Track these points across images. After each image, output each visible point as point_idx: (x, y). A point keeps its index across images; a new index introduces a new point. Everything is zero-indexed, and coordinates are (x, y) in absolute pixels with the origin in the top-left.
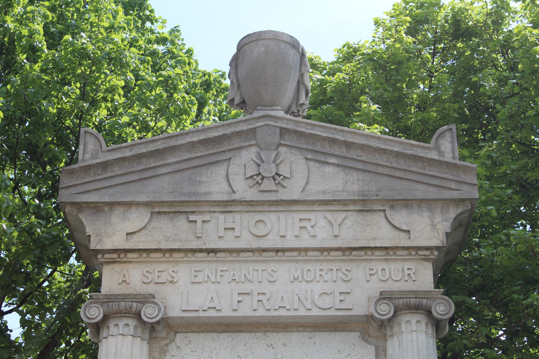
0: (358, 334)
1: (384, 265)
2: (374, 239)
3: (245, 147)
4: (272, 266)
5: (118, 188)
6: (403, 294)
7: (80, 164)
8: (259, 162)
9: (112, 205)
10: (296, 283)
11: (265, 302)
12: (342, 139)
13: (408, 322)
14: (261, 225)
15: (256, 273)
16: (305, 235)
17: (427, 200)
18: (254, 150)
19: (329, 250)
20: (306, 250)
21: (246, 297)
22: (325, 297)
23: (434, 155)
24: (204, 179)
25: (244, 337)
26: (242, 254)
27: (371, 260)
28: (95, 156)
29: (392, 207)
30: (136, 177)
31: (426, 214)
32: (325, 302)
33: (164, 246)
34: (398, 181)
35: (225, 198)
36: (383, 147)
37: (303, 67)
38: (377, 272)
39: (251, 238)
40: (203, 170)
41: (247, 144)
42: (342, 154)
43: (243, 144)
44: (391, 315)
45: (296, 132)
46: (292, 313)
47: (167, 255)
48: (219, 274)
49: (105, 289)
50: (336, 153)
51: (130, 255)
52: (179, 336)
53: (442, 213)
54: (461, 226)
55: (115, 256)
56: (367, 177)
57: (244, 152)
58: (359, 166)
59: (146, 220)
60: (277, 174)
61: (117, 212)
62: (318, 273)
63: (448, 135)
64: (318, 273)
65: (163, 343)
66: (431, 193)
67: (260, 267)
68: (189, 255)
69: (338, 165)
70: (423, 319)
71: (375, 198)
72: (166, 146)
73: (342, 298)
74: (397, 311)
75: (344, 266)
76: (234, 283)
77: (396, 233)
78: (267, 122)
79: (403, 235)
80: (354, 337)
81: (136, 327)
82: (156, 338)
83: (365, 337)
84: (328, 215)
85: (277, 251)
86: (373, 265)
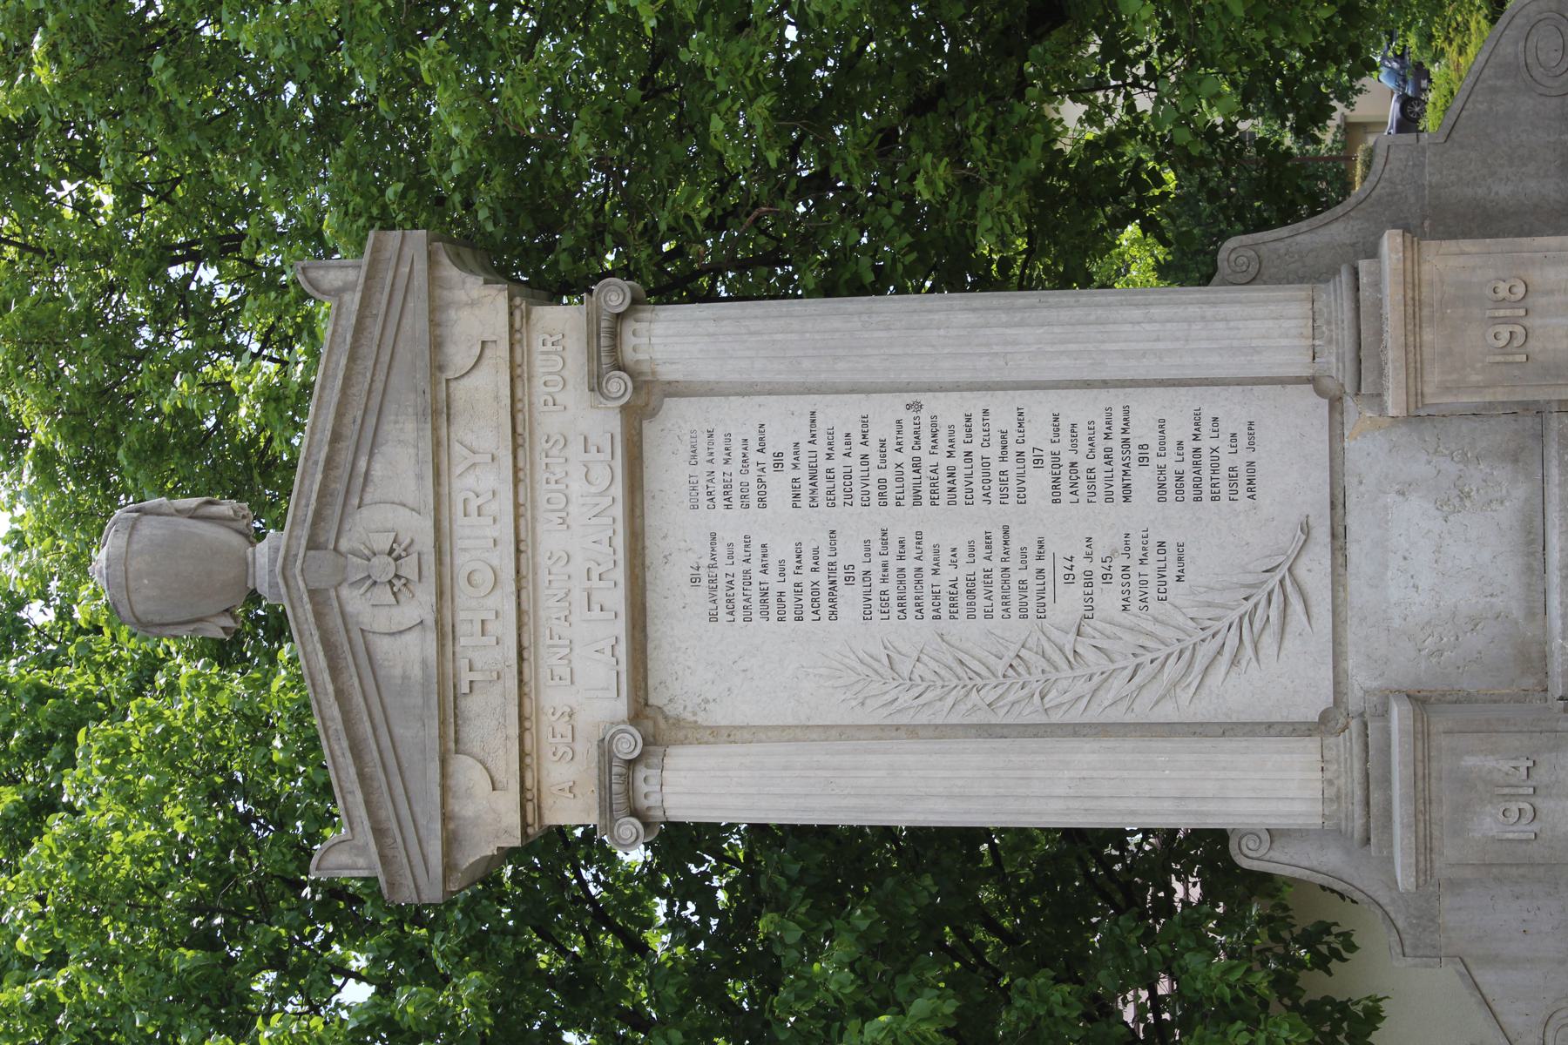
0: (645, 424)
1: (538, 382)
2: (497, 398)
3: (341, 606)
4: (543, 560)
5: (417, 809)
6: (594, 355)
7: (379, 872)
8: (369, 582)
9: (446, 818)
10: (568, 521)
11: (602, 569)
12: (326, 449)
13: (635, 349)
14: (477, 578)
15: (554, 585)
18: (345, 592)
19: (516, 470)
20: (517, 505)
21: (593, 599)
23: (353, 301)
24: (398, 672)
26: (524, 606)
27: (530, 404)
28: (362, 850)
29: (441, 368)
30: (397, 781)
31: (452, 313)
32: (601, 475)
33: (514, 731)
34: (398, 357)
35: (432, 637)
36: (339, 382)
37: (163, 510)
38: (549, 394)
39: (498, 592)
40: (381, 673)
41: (335, 604)
42: (352, 448)
43: (337, 610)
44: (625, 376)
45: (314, 524)
46: (620, 527)
47: (527, 724)
48: (556, 641)
49: (593, 820)
50: (350, 457)
51: (529, 783)
52: (652, 700)
53: (451, 289)
54: (458, 255)
55: (530, 807)
56: (390, 408)
57: (349, 609)
58: (372, 421)
59: (470, 761)
60: (390, 554)
61: (457, 808)
62: (553, 486)
63: (313, 274)
65: (662, 723)
66: (418, 305)
67: (543, 577)
68: (526, 690)
69: (371, 455)
70: (629, 327)
71: (428, 396)
72: (343, 736)
73: (594, 449)
74: (619, 366)
75: (541, 445)
76: (571, 618)
77: (485, 362)
78: (297, 571)
79: (488, 352)
80: (650, 430)
81: (647, 766)
82: (654, 736)
84: (457, 470)
85: (518, 551)
86: (538, 401)
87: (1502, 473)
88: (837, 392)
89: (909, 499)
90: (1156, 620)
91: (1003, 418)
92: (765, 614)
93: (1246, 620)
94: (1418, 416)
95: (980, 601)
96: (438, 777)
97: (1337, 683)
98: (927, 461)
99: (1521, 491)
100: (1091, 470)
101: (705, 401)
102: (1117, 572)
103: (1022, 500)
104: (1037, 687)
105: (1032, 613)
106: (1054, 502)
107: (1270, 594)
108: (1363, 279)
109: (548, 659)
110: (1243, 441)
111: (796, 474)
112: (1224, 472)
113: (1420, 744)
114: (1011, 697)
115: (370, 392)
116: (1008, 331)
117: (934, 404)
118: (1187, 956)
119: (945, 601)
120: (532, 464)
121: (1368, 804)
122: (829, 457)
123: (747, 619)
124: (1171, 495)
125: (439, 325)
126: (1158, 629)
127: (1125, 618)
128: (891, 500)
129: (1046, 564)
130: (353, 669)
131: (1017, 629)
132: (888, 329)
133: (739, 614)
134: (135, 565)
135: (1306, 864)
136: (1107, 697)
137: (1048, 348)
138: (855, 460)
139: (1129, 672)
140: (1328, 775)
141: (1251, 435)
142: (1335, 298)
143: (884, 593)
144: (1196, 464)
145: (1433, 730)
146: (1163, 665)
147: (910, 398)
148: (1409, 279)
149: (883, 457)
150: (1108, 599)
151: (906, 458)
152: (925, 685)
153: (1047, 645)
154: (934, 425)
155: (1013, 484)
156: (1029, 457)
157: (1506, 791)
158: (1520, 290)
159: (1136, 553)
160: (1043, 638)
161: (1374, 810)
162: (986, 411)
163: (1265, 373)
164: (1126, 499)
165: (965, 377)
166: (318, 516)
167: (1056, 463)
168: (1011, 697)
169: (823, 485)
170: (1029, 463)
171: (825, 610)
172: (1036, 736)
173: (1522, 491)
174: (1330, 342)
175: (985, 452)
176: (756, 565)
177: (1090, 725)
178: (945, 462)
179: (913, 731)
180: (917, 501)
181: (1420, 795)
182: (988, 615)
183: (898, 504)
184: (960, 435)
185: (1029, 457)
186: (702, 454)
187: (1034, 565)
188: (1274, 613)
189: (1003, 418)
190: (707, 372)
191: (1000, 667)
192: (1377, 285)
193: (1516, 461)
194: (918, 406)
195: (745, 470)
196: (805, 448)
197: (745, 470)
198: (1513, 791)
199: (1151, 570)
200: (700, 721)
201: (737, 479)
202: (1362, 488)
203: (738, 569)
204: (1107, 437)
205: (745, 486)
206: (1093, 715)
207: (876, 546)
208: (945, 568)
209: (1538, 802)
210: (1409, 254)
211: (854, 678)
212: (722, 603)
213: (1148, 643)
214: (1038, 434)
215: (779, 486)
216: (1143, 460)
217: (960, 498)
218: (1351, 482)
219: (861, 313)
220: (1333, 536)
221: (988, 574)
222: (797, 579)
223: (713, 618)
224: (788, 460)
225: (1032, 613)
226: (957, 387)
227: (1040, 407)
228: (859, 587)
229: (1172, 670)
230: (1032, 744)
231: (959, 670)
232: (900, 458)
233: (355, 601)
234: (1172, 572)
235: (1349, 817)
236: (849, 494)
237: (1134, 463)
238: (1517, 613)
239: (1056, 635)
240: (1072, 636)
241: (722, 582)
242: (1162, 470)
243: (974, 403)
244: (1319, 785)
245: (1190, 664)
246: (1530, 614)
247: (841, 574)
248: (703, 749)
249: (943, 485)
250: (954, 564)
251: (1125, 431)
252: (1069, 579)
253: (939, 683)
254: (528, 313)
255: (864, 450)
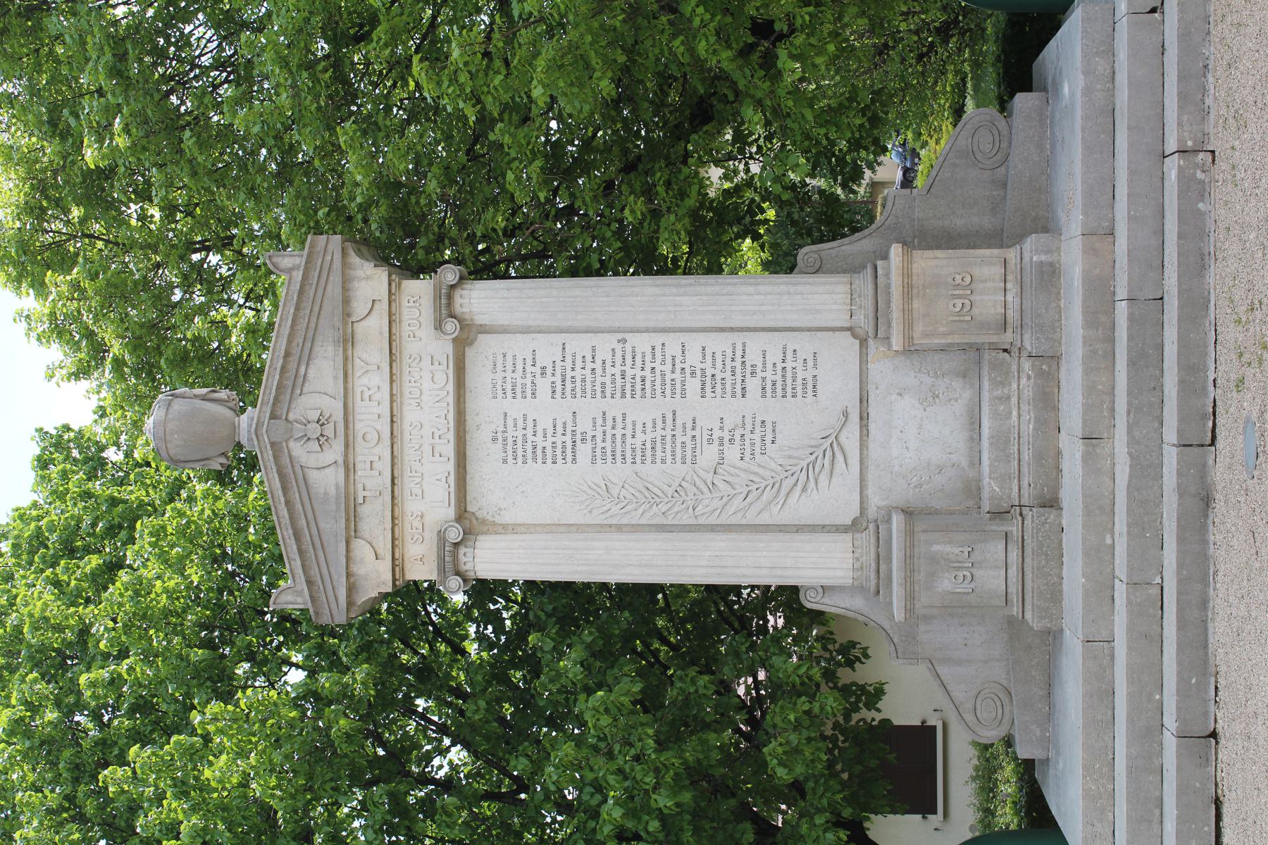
0: (467, 349)
1: (405, 324)
2: (381, 333)
6: (437, 308)
7: (309, 606)
8: (306, 438)
9: (348, 575)
10: (422, 404)
11: (440, 433)
13: (461, 306)
14: (368, 437)
15: (413, 441)
16: (377, 396)
17: (344, 282)
18: (292, 444)
20: (392, 395)
21: (435, 450)
22: (436, 378)
23: (298, 275)
24: (322, 490)
25: (470, 452)
26: (395, 454)
28: (300, 593)
29: (349, 315)
30: (321, 554)
31: (356, 284)
34: (324, 308)
35: (342, 471)
36: (289, 322)
37: (187, 395)
39: (380, 445)
40: (312, 491)
41: (286, 451)
42: (297, 360)
43: (287, 454)
45: (274, 404)
46: (451, 408)
47: (396, 522)
48: (414, 474)
49: (434, 577)
50: (295, 366)
51: (397, 556)
54: (359, 250)
55: (397, 569)
56: (319, 338)
57: (294, 454)
58: (308, 345)
59: (363, 542)
61: (355, 570)
62: (413, 384)
63: (275, 260)
64: (413, 384)
65: (474, 522)
66: (336, 278)
67: (407, 437)
69: (308, 365)
70: (457, 293)
71: (341, 331)
72: (289, 527)
73: (437, 363)
75: (406, 360)
76: (422, 461)
77: (374, 312)
78: (264, 431)
79: (376, 306)
80: (470, 352)
81: (466, 547)
83: (471, 343)
84: (358, 374)
85: (392, 421)
86: (405, 335)
87: (957, 384)
88: (578, 332)
89: (618, 394)
90: (759, 465)
91: (673, 349)
92: (535, 459)
93: (811, 466)
94: (910, 350)
95: (659, 454)
96: (344, 552)
97: (862, 503)
98: (629, 373)
99: (967, 394)
100: (723, 379)
101: (502, 336)
102: (737, 438)
103: (683, 396)
104: (691, 503)
105: (688, 460)
106: (702, 397)
107: (825, 451)
108: (880, 272)
109: (409, 484)
110: (810, 363)
111: (553, 379)
112: (799, 381)
113: (908, 538)
114: (676, 509)
115: (307, 328)
116: (677, 298)
117: (635, 340)
118: (774, 658)
119: (639, 453)
120: (401, 371)
121: (878, 572)
122: (573, 369)
123: (525, 462)
124: (769, 394)
125: (348, 290)
126: (760, 471)
127: (740, 464)
128: (608, 394)
129: (697, 433)
130: (295, 488)
131: (679, 470)
132: (608, 296)
133: (520, 459)
134: (170, 426)
135: (843, 606)
136: (731, 509)
137: (699, 309)
138: (588, 372)
139: (743, 495)
140: (856, 555)
141: (815, 360)
142: (864, 283)
143: (603, 448)
144: (783, 376)
145: (916, 529)
146: (763, 492)
147: (620, 336)
148: (906, 272)
149: (604, 370)
150: (732, 453)
151: (617, 371)
152: (626, 501)
153: (697, 479)
154: (634, 352)
155: (678, 386)
156: (688, 371)
157: (956, 565)
158: (968, 279)
159: (749, 427)
160: (695, 475)
161: (882, 575)
162: (663, 344)
163: (823, 324)
164: (743, 396)
165: (652, 324)
166: (276, 400)
167: (704, 375)
168: (676, 509)
169: (569, 386)
170: (688, 374)
171: (569, 458)
172: (690, 531)
173: (967, 394)
174: (861, 307)
175: (663, 368)
176: (530, 431)
177: (721, 525)
178: (639, 374)
179: (619, 528)
180: (623, 395)
181: (908, 567)
182: (664, 461)
183: (612, 397)
184: (648, 358)
185: (688, 371)
186: (499, 367)
187: (690, 433)
188: (827, 462)
189: (673, 349)
190: (503, 319)
191: (670, 492)
192: (887, 275)
193: (965, 377)
194: (624, 341)
195: (524, 377)
196: (559, 364)
197: (524, 377)
198: (960, 565)
199: (757, 437)
200: (496, 520)
201: (519, 381)
202: (878, 391)
203: (520, 433)
204: (733, 360)
205: (524, 385)
206: (723, 520)
207: (599, 421)
208: (639, 434)
209: (974, 571)
210: (906, 257)
211: (586, 497)
212: (510, 453)
213: (754, 479)
214: (693, 358)
215: (544, 385)
216: (753, 373)
217: (648, 394)
218: (871, 387)
219: (592, 287)
220: (861, 418)
221: (663, 438)
222: (554, 439)
223: (505, 461)
224: (549, 371)
225: (688, 460)
226: (647, 330)
227: (695, 342)
228: (589, 445)
229: (768, 494)
230: (688, 536)
231: (646, 493)
232: (614, 370)
233: (297, 449)
234: (769, 438)
235: (868, 579)
236: (584, 391)
237: (748, 376)
238: (964, 463)
239: (702, 473)
240: (711, 474)
241: (510, 441)
242: (764, 379)
243: (657, 339)
244: (851, 561)
245: (779, 491)
246: (972, 464)
247: (579, 437)
248: (498, 537)
249: (638, 387)
250: (644, 432)
251: (743, 357)
252: (710, 441)
253: (635, 500)
254: (400, 284)
255: (593, 366)
